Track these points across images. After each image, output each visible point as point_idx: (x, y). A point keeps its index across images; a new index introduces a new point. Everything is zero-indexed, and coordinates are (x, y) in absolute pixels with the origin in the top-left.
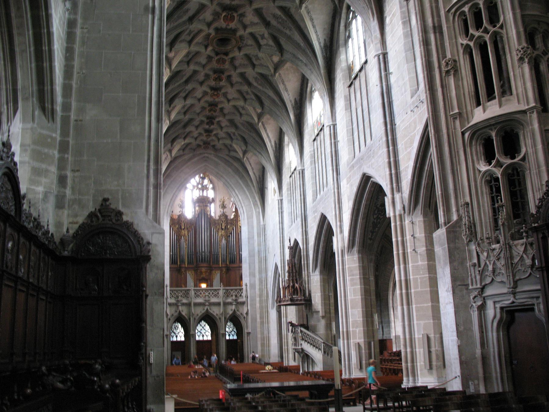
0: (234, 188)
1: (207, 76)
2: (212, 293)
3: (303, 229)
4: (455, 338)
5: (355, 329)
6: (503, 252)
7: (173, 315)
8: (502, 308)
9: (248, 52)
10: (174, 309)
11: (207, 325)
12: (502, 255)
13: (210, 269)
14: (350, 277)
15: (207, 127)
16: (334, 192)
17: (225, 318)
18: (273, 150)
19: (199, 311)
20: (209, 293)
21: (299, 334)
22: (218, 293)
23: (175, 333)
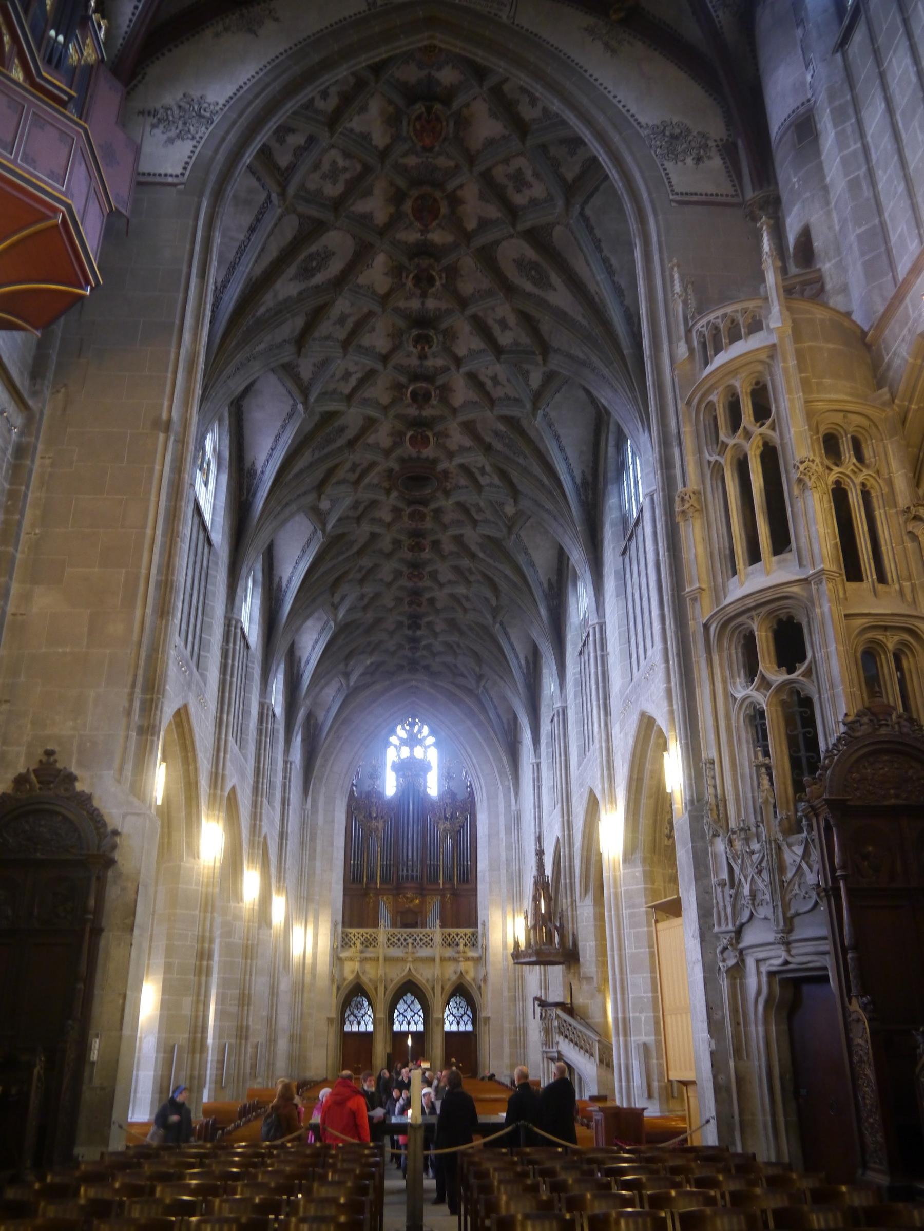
1: (397, 543)
2: (421, 940)
3: (563, 817)
4: (706, 1035)
5: (637, 1014)
6: (766, 858)
8: (771, 974)
9: (462, 498)
11: (416, 1001)
12: (764, 864)
14: (629, 911)
15: (410, 633)
16: (601, 747)
17: (443, 988)
18: (523, 674)
19: (397, 975)
20: (415, 940)
21: (554, 1022)
23: (356, 1017)
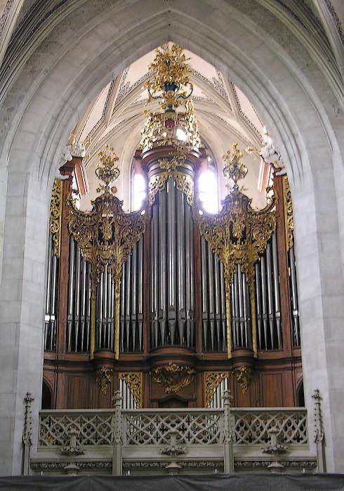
0: (266, 78)
2: (195, 429)
13: (197, 366)
20: (184, 430)
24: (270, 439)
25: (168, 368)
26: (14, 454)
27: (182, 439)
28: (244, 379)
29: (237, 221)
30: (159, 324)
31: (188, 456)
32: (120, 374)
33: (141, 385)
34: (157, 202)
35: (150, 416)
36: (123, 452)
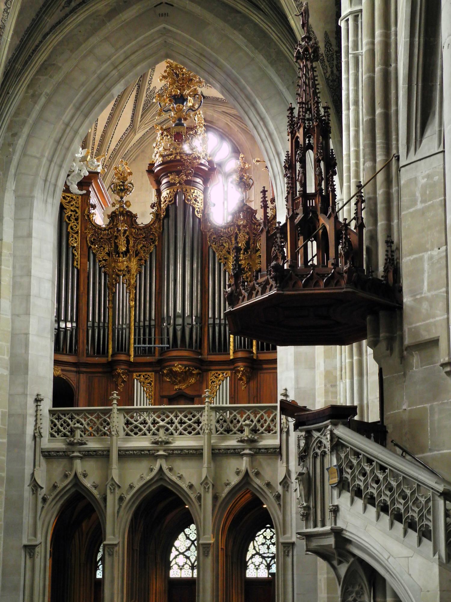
2: (181, 423)
7: (55, 487)
10: (59, 467)
17: (215, 498)
20: (171, 423)
21: (327, 459)
22: (198, 422)
24: (244, 430)
25: (174, 369)
26: (27, 446)
27: (170, 431)
28: (244, 378)
29: (242, 232)
30: (168, 330)
31: (173, 445)
32: (135, 374)
33: (153, 384)
34: (167, 216)
35: (170, 412)
36: (119, 442)
